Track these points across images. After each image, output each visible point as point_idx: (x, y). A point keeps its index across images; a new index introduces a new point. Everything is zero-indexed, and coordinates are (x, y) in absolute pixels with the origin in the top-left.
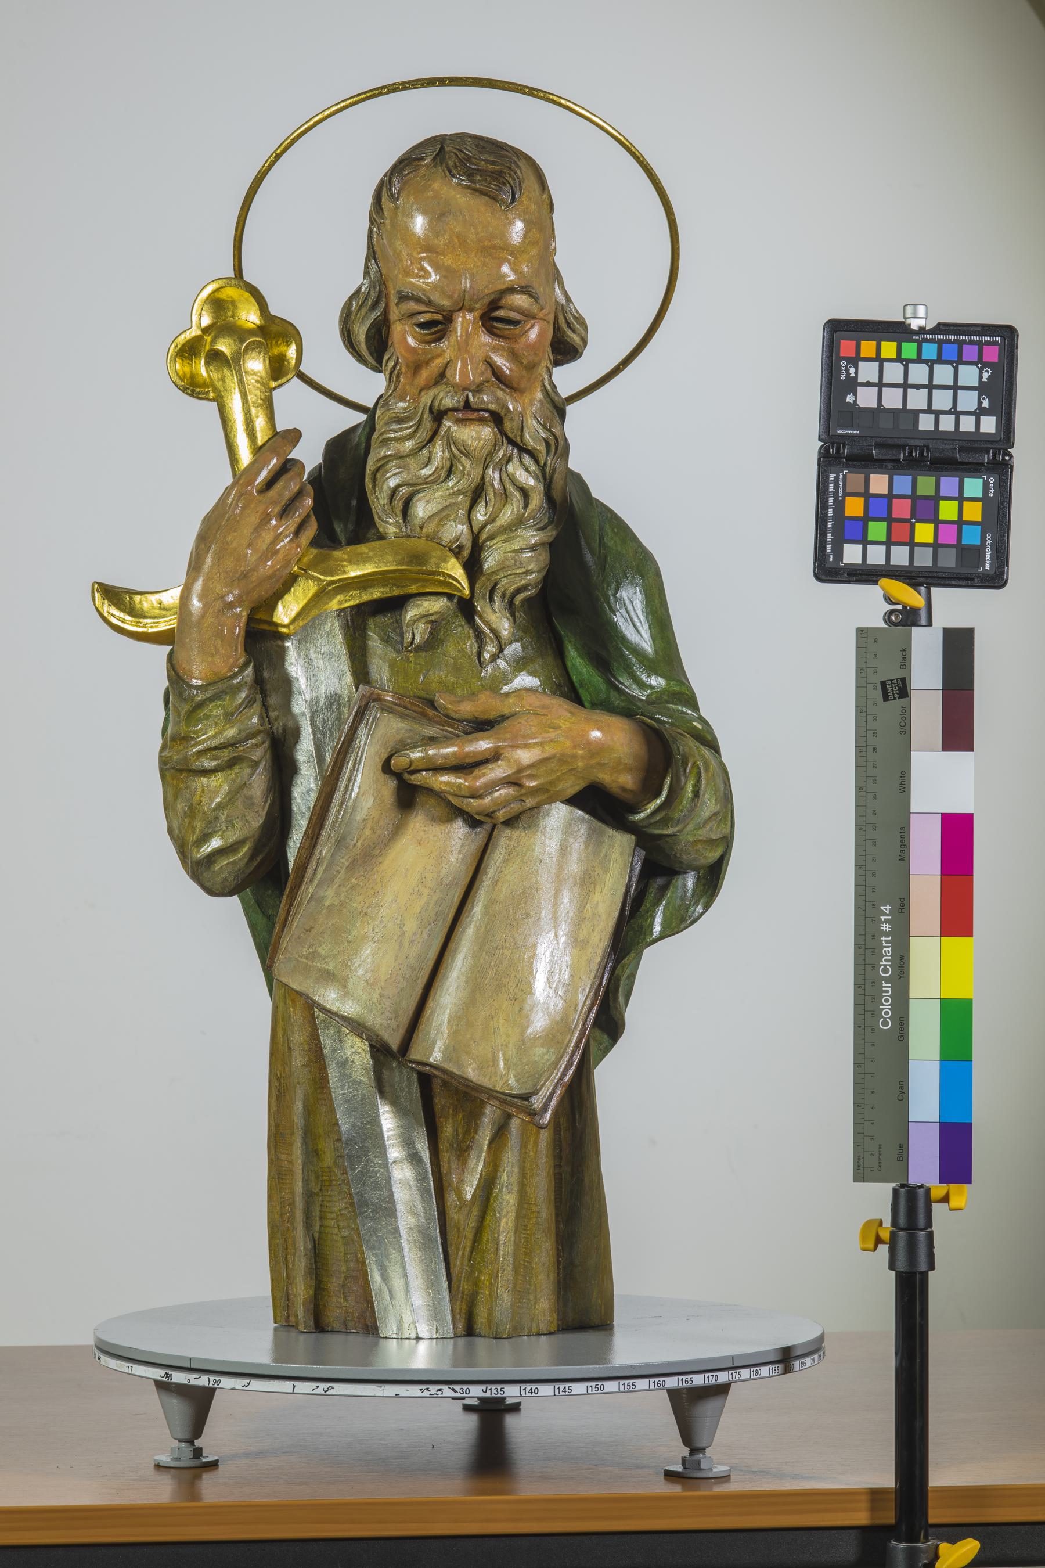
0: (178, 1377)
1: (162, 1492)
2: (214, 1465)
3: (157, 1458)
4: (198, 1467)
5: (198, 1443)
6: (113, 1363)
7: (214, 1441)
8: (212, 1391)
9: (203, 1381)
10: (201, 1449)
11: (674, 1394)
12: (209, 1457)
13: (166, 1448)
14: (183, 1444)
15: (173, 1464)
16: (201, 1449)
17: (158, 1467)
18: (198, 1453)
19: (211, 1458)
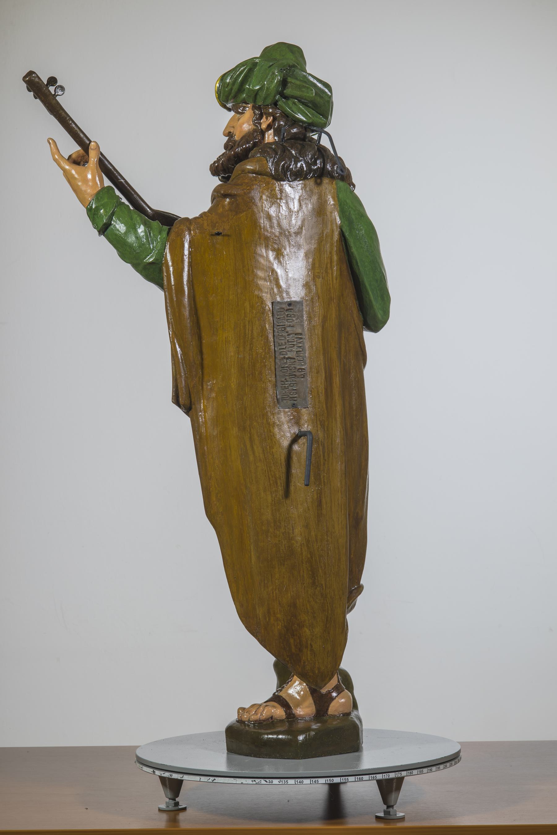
2: (184, 809)
5: (177, 799)
7: (182, 800)
15: (168, 809)
16: (178, 802)
19: (184, 806)
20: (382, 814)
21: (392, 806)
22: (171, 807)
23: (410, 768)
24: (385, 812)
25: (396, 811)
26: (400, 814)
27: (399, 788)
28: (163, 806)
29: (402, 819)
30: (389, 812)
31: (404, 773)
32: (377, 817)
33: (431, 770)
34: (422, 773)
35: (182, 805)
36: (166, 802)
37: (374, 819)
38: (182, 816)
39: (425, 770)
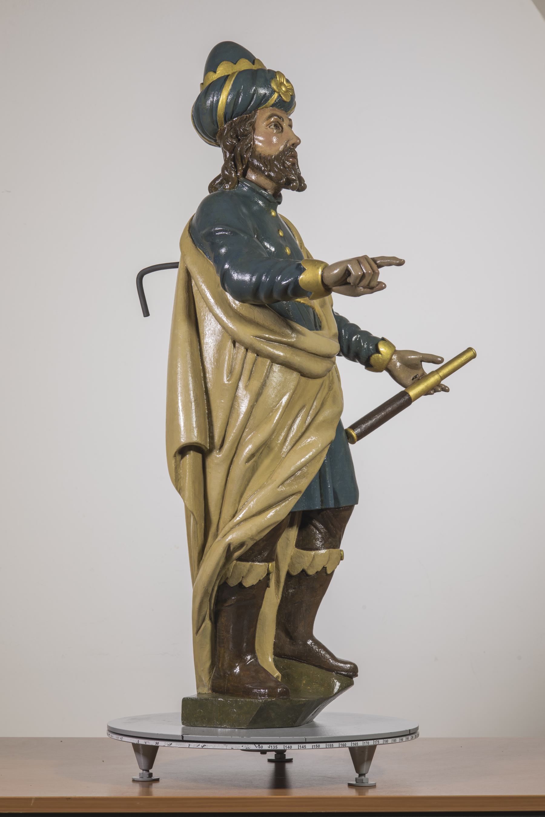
0: (142, 742)
1: (135, 791)
2: (157, 780)
3: (134, 777)
4: (150, 781)
5: (151, 771)
6: (115, 736)
8: (155, 749)
9: (152, 743)
10: (152, 774)
11: (351, 749)
12: (155, 777)
13: (137, 772)
14: (145, 772)
16: (152, 774)
17: (134, 781)
18: (151, 775)
20: (354, 783)
21: (364, 775)
22: (146, 778)
23: (386, 737)
24: (356, 779)
25: (368, 779)
26: (371, 782)
27: (370, 758)
28: (137, 777)
29: (374, 786)
30: (362, 780)
31: (381, 741)
32: (350, 785)
33: (402, 740)
34: (395, 742)
35: (155, 777)
36: (140, 774)
37: (347, 786)
38: (155, 785)
39: (398, 740)
